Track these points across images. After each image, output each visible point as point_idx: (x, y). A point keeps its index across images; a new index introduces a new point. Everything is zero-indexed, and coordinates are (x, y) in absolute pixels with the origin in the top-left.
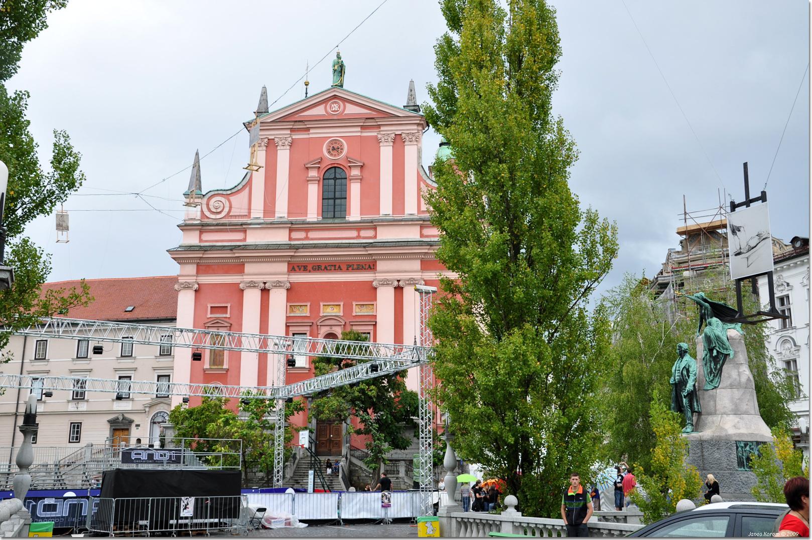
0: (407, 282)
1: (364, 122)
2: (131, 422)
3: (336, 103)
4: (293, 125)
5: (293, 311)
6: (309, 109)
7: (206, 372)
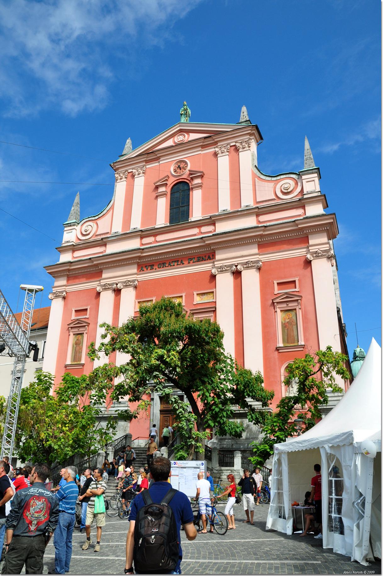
0: (245, 266)
1: (203, 142)
3: (181, 135)
4: (147, 157)
6: (160, 144)
7: (67, 368)
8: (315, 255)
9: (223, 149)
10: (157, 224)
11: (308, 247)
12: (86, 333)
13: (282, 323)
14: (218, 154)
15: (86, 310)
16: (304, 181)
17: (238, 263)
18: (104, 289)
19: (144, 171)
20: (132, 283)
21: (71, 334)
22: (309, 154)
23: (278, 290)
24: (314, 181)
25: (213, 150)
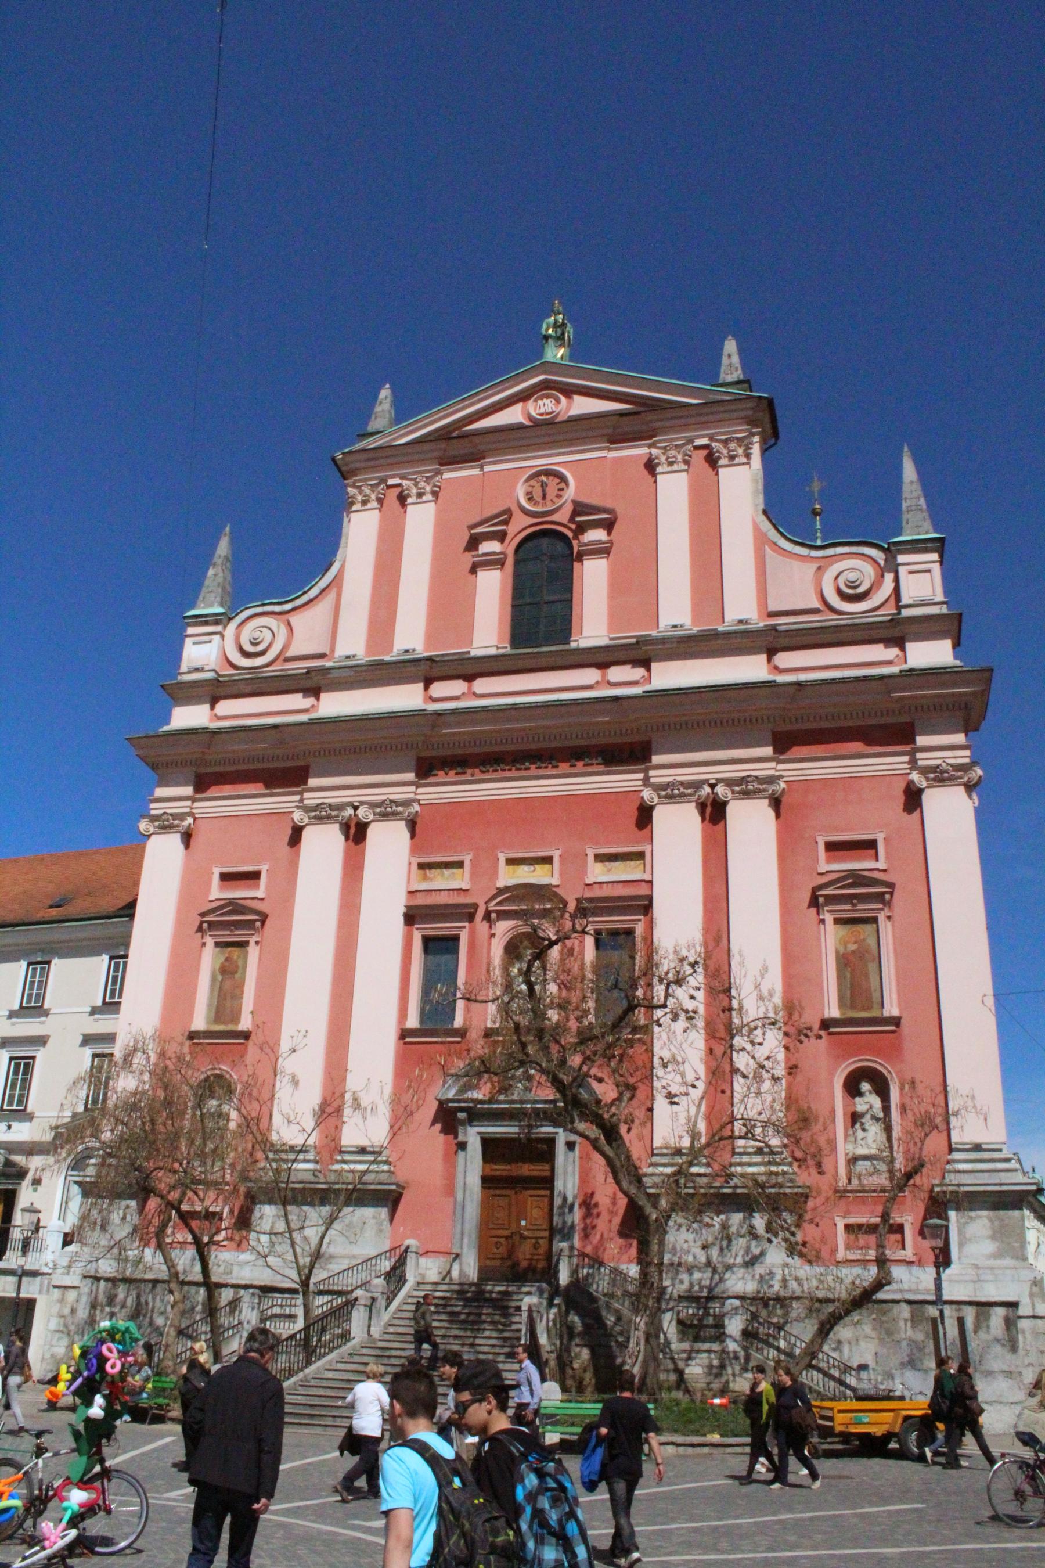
2: (22, 1174)
3: (548, 397)
5: (425, 878)
8: (932, 776)
9: (673, 452)
10: (475, 645)
11: (912, 754)
12: (257, 943)
13: (837, 952)
14: (658, 464)
15: (255, 875)
16: (902, 571)
17: (717, 779)
18: (315, 818)
19: (435, 486)
20: (400, 809)
21: (210, 941)
22: (915, 494)
23: (829, 861)
24: (929, 571)
25: (645, 451)
